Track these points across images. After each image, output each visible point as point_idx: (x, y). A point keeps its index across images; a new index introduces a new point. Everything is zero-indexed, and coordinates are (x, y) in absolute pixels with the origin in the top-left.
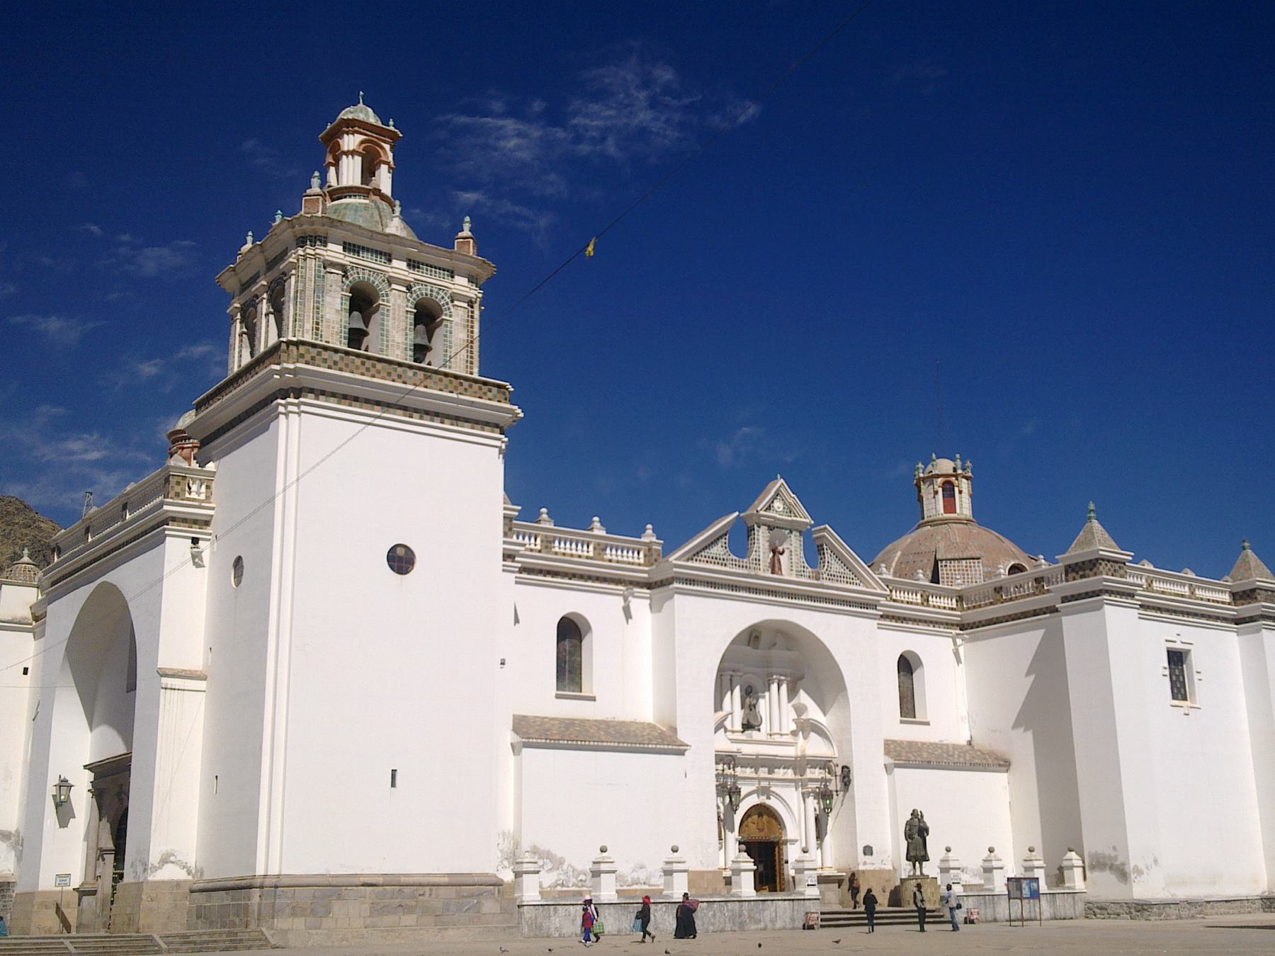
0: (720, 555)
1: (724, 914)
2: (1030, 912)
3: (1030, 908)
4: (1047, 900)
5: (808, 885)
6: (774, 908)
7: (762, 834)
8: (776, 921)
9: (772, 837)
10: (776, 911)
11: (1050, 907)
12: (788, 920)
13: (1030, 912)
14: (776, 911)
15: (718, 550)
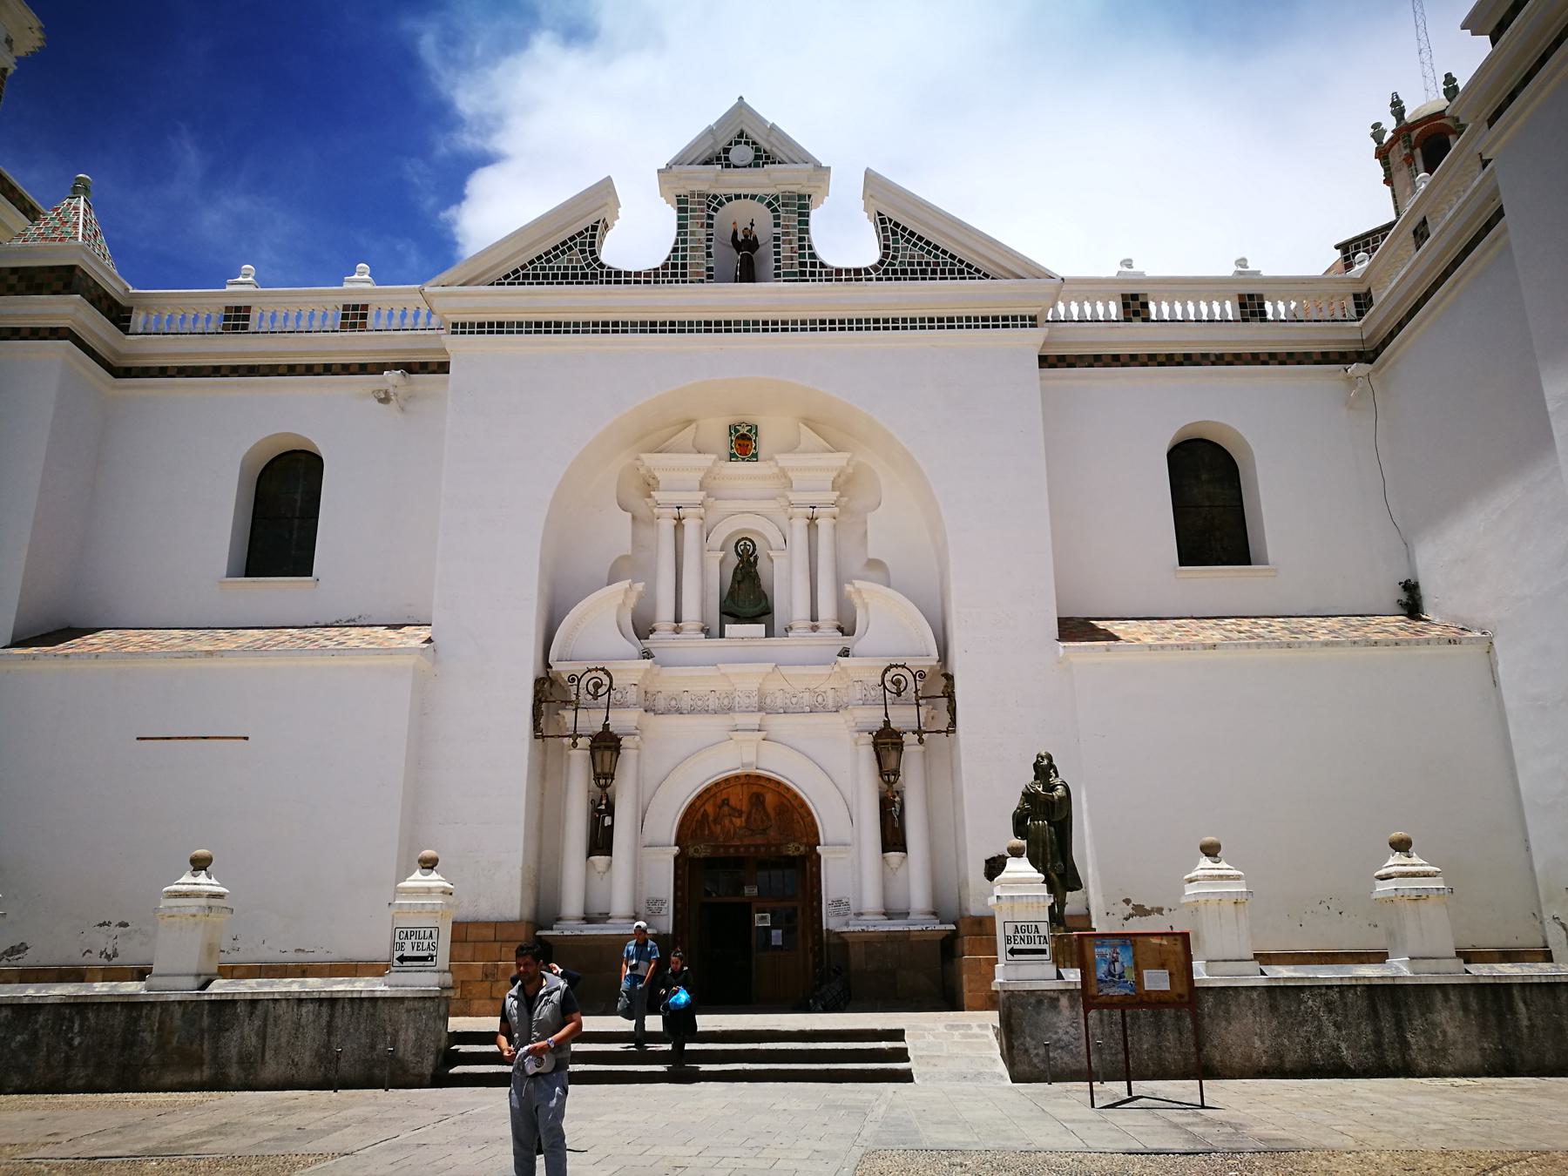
0: (574, 268)
1: (69, 1043)
2: (1378, 1045)
3: (1378, 1032)
4: (1465, 1008)
5: (402, 959)
6: (257, 1023)
7: (759, 840)
8: (263, 1062)
9: (791, 850)
10: (262, 1035)
11: (1484, 1030)
12: (308, 1058)
13: (1378, 1045)
14: (262, 1035)
15: (570, 261)
